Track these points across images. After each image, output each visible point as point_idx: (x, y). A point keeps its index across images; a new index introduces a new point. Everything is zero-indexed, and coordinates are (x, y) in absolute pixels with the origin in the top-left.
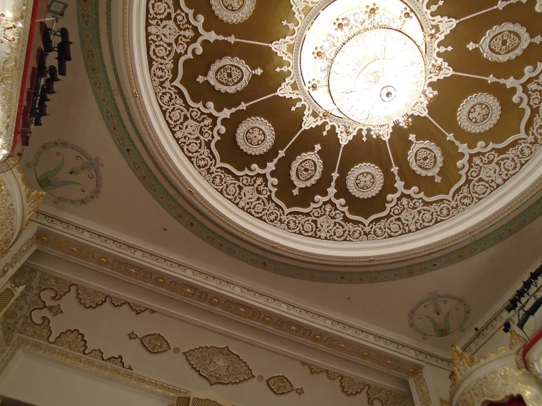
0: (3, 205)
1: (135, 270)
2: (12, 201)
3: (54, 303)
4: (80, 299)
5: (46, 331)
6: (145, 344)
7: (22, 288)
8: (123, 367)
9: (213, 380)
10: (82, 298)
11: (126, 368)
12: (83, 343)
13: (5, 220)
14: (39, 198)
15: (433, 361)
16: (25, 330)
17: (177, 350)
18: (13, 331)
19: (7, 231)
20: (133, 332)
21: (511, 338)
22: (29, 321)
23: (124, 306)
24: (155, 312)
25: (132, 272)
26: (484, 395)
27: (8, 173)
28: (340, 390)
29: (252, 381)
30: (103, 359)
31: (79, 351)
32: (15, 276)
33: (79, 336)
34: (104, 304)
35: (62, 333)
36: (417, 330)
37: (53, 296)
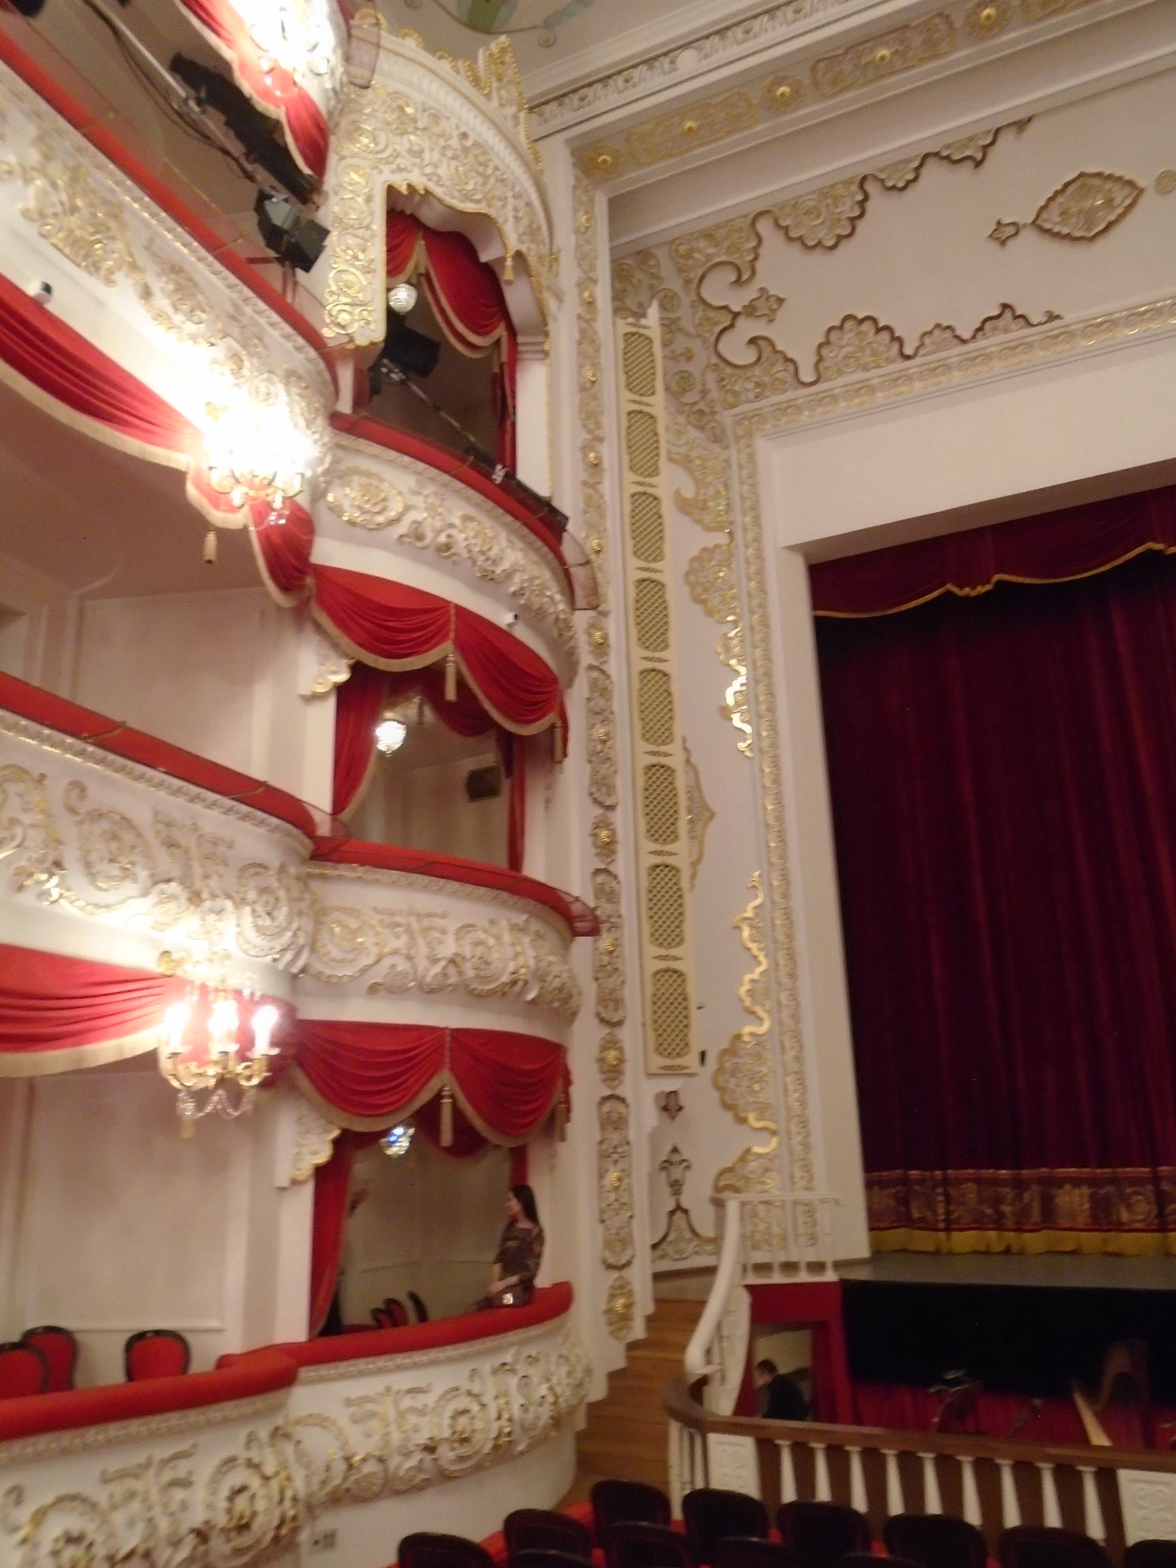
0: (449, 153)
1: (886, 45)
2: (458, 127)
4: (801, 239)
5: (779, 366)
6: (1056, 229)
7: (653, 314)
8: (1030, 325)
10: (803, 232)
11: (1040, 324)
12: (885, 336)
13: (484, 184)
14: (503, 63)
16: (736, 394)
18: (713, 413)
19: (509, 208)
20: (999, 223)
22: (729, 370)
23: (925, 172)
24: (1030, 119)
25: (883, 58)
27: (385, 62)
30: (964, 342)
31: (889, 361)
32: (618, 297)
33: (867, 327)
34: (869, 206)
35: (820, 346)
37: (734, 278)
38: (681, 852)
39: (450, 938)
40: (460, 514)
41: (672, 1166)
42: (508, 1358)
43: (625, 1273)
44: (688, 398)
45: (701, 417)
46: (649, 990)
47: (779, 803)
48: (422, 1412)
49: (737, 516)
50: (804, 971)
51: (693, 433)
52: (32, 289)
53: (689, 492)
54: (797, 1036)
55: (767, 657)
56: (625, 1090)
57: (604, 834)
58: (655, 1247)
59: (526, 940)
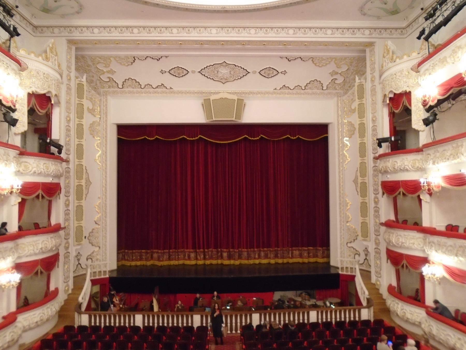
3: (109, 69)
5: (114, 84)
7: (85, 77)
9: (224, 81)
15: (385, 34)
17: (193, 72)
19: (53, 86)
21: (422, 44)
26: (391, 87)
28: (314, 65)
29: (248, 75)
31: (138, 88)
33: (133, 81)
35: (123, 82)
36: (370, 16)
38: (83, 203)
40: (42, 164)
41: (78, 257)
42: (48, 306)
44: (92, 84)
45: (95, 89)
47: (106, 181)
48: (35, 318)
49: (102, 114)
50: (108, 215)
51: (93, 92)
53: (91, 107)
54: (106, 229)
55: (106, 148)
57: (67, 203)
58: (74, 272)
59: (53, 239)
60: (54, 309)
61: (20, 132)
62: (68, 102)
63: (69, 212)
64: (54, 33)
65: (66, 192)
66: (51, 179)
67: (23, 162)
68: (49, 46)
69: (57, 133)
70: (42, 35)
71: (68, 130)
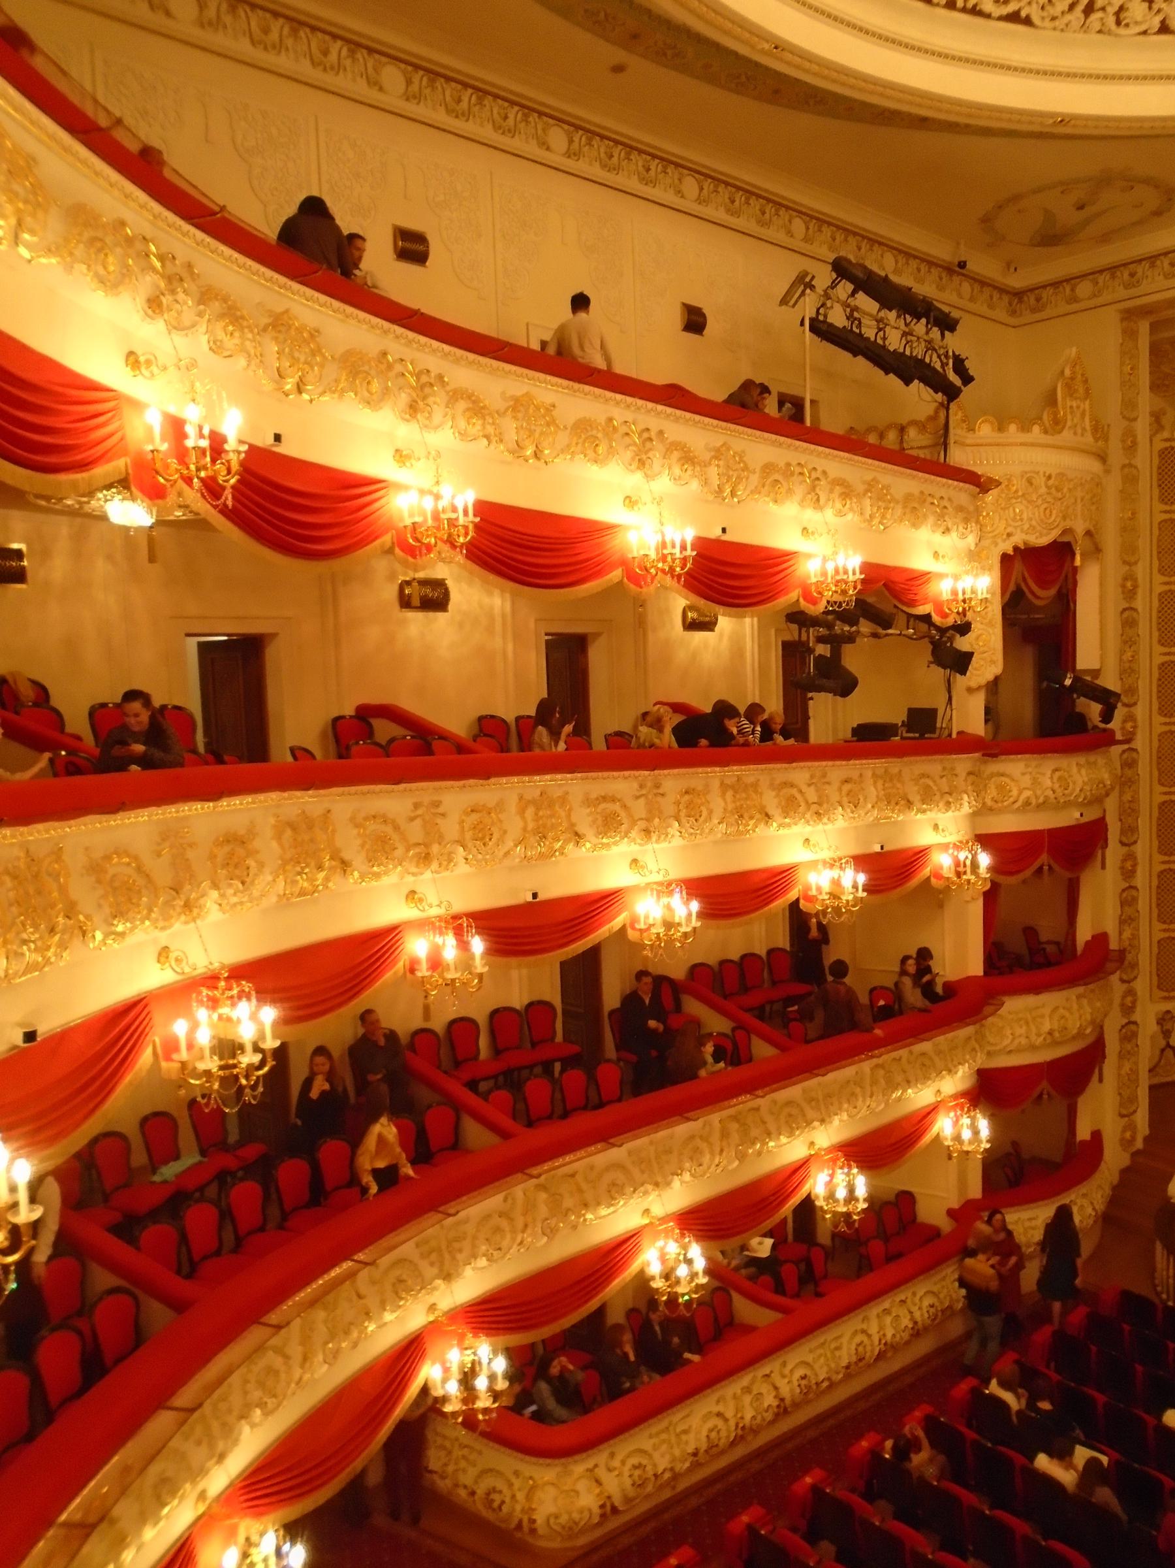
19: (1079, 506)
39: (1048, 1019)
40: (1049, 773)
43: (1132, 1117)
46: (1155, 950)
48: (1033, 1228)
52: (877, 849)
56: (1136, 1017)
57: (1128, 865)
58: (1150, 1071)
59: (1085, 1002)
60: (1090, 1210)
61: (983, 681)
62: (1128, 528)
63: (1134, 893)
64: (1074, 299)
65: (1123, 832)
66: (1077, 815)
67: (992, 775)
68: (1062, 372)
69: (1093, 648)
70: (1038, 316)
71: (1128, 622)
